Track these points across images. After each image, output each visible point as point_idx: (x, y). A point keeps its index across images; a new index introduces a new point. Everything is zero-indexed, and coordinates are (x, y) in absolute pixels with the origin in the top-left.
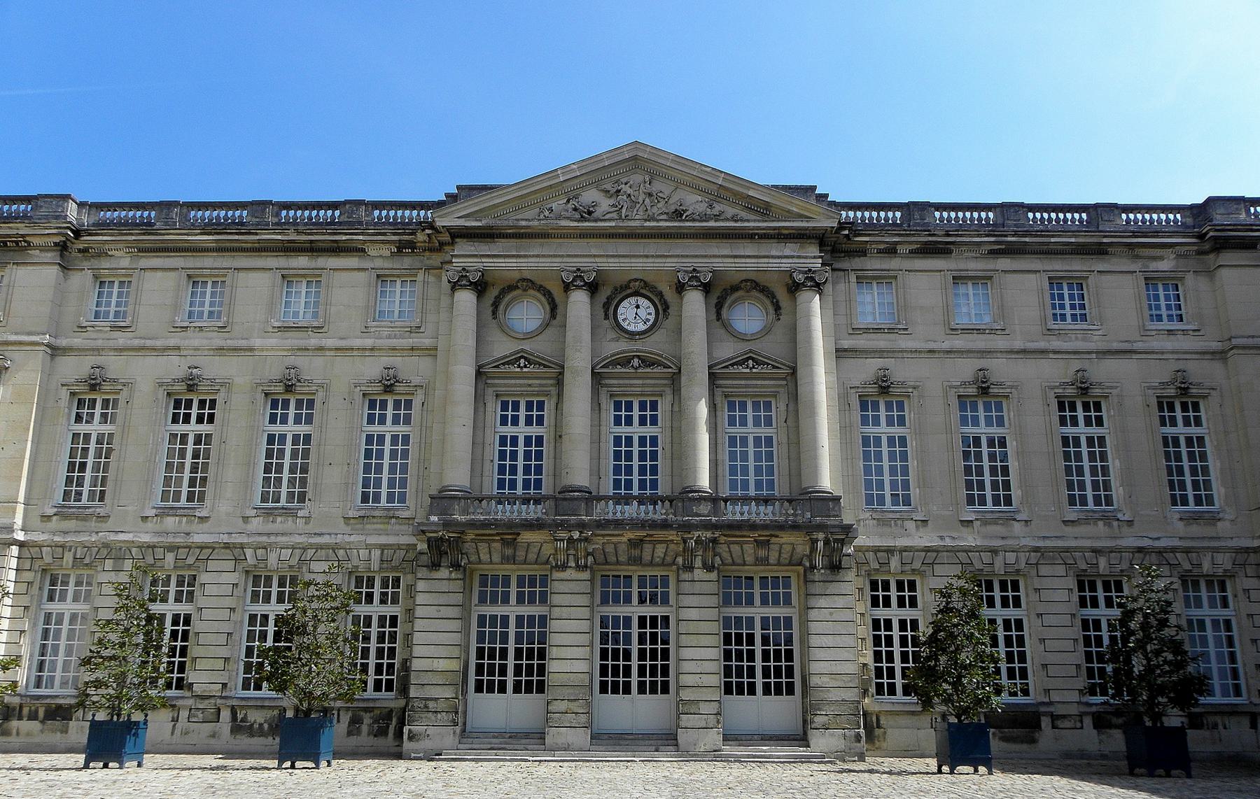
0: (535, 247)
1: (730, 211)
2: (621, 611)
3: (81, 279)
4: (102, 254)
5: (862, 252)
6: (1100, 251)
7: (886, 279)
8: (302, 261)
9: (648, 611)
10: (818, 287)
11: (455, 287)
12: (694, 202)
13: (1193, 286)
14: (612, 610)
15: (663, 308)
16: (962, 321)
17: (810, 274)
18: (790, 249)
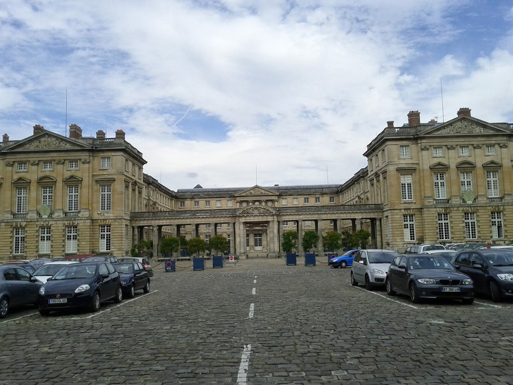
0: (246, 198)
1: (267, 192)
2: (256, 238)
3: (193, 202)
4: (195, 198)
5: (283, 195)
6: (310, 195)
7: (286, 199)
8: (218, 199)
9: (259, 238)
10: (277, 201)
11: (237, 203)
12: (263, 191)
13: (321, 198)
14: (256, 238)
15: (260, 203)
16: (295, 203)
17: (276, 200)
18: (274, 197)
